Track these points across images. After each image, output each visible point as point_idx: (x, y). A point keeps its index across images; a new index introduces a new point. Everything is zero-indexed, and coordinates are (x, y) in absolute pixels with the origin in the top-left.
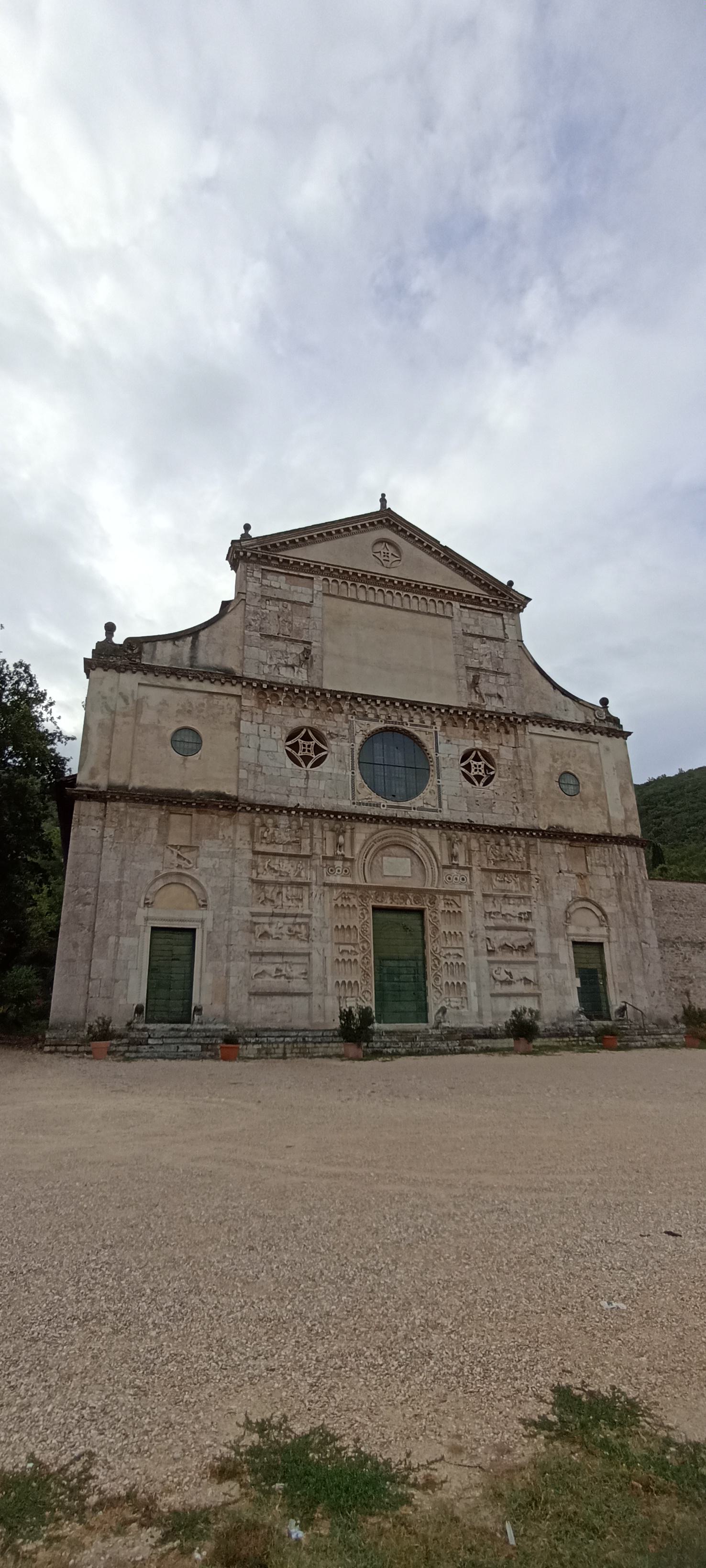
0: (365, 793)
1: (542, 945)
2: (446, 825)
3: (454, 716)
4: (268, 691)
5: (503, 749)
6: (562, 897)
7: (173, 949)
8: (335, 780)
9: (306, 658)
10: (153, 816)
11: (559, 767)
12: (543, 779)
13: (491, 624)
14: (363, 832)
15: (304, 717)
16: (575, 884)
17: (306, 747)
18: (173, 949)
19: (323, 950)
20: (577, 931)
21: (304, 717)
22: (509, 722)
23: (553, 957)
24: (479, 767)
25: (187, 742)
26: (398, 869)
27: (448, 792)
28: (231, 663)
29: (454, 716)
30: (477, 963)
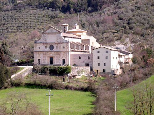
0: (50, 50)
1: (60, 60)
2: (54, 52)
3: (55, 43)
4: (44, 44)
5: (59, 45)
6: (62, 56)
7: (39, 60)
8: (48, 49)
9: (46, 40)
10: (38, 53)
11: (63, 46)
12: (62, 47)
13: (59, 35)
14: (49, 53)
15: (46, 45)
16: (63, 55)
17: (46, 47)
18: (39, 60)
19: (47, 60)
20: (63, 59)
21: (46, 45)
22: (59, 43)
23: (61, 60)
24: (57, 47)
25: (39, 48)
26: (51, 55)
27: (55, 49)
28: (41, 42)
29: (55, 43)
30: (56, 61)
